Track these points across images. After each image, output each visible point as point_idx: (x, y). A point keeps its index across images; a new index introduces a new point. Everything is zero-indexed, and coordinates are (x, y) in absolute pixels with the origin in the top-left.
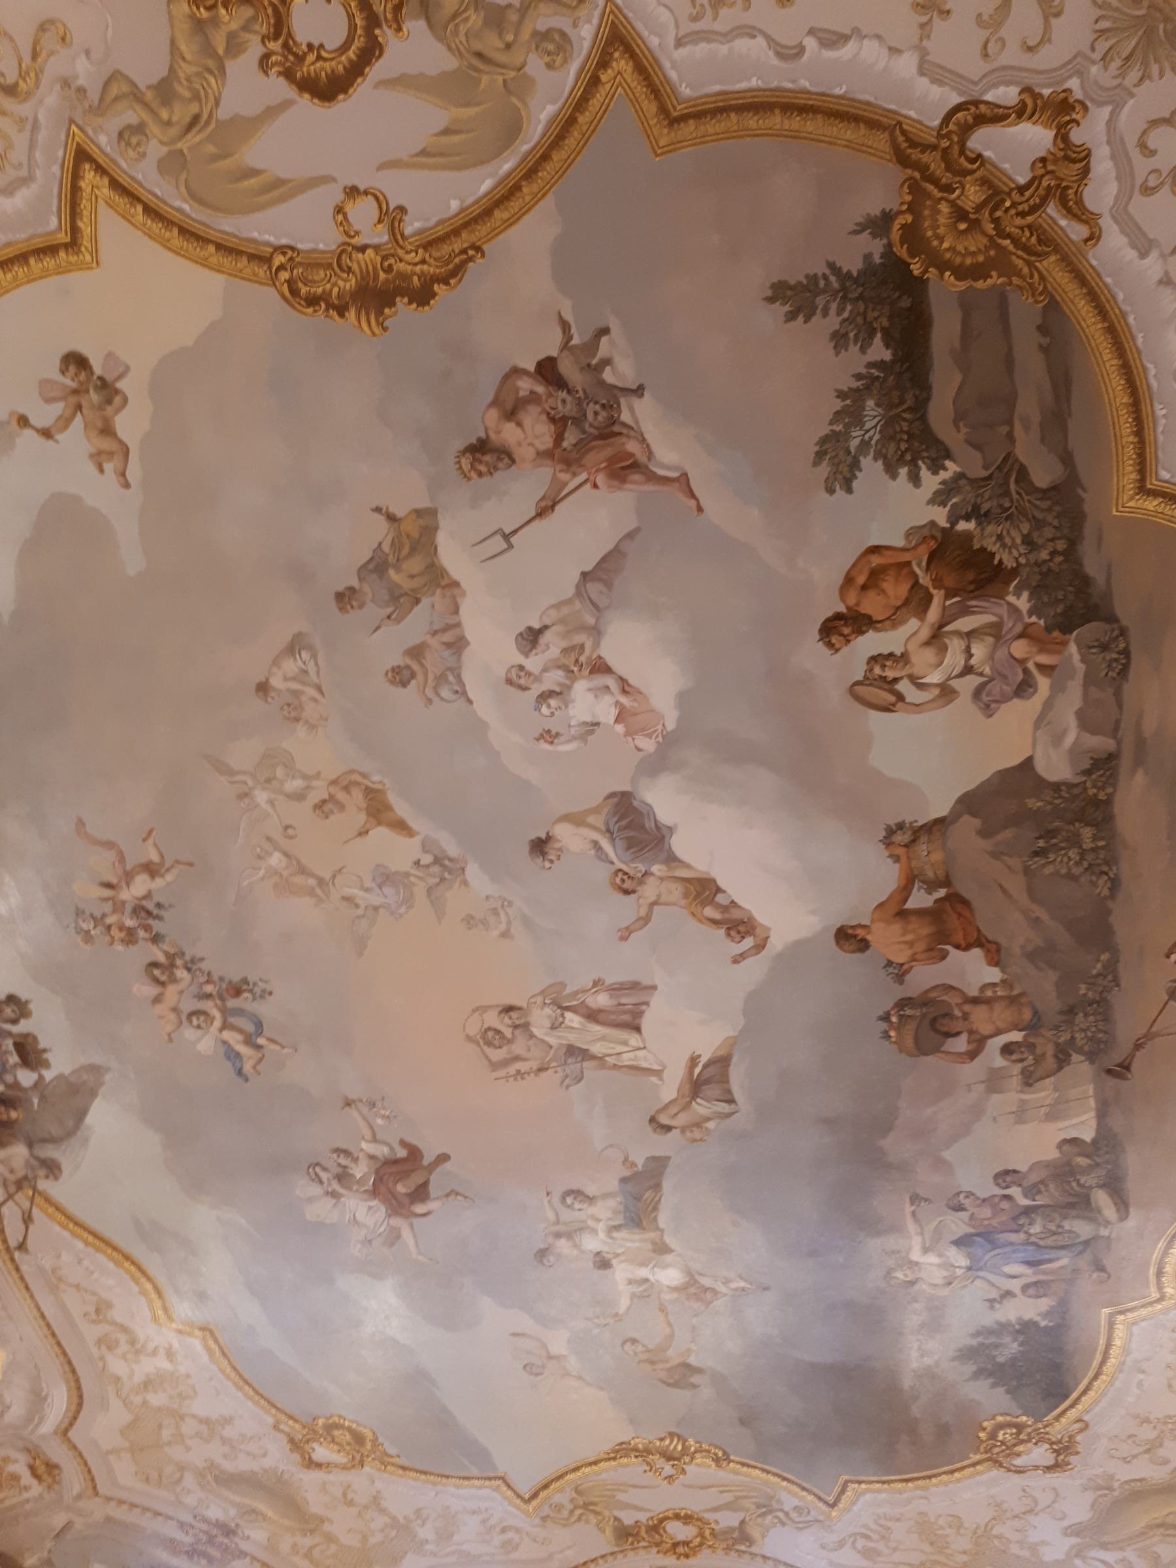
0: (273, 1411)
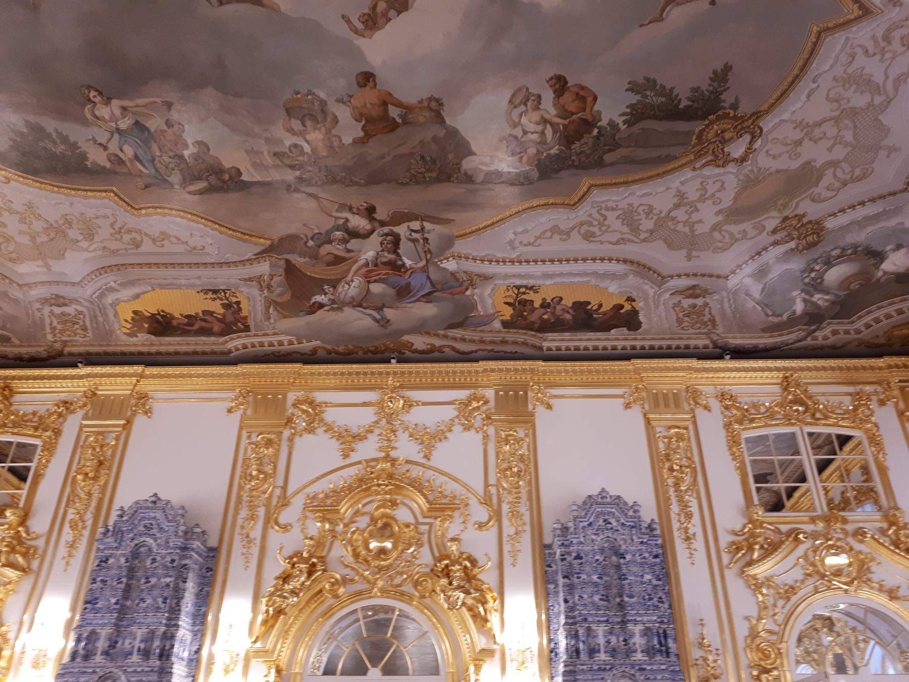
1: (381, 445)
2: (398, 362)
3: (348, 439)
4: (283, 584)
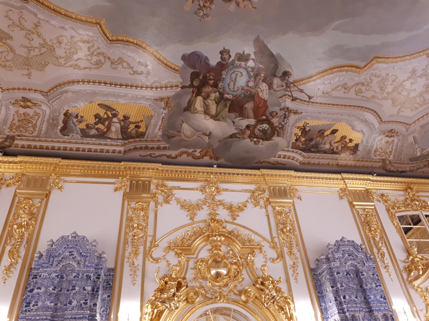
0: (422, 54)
1: (210, 212)
2: (218, 167)
3: (190, 208)
4: (161, 295)
